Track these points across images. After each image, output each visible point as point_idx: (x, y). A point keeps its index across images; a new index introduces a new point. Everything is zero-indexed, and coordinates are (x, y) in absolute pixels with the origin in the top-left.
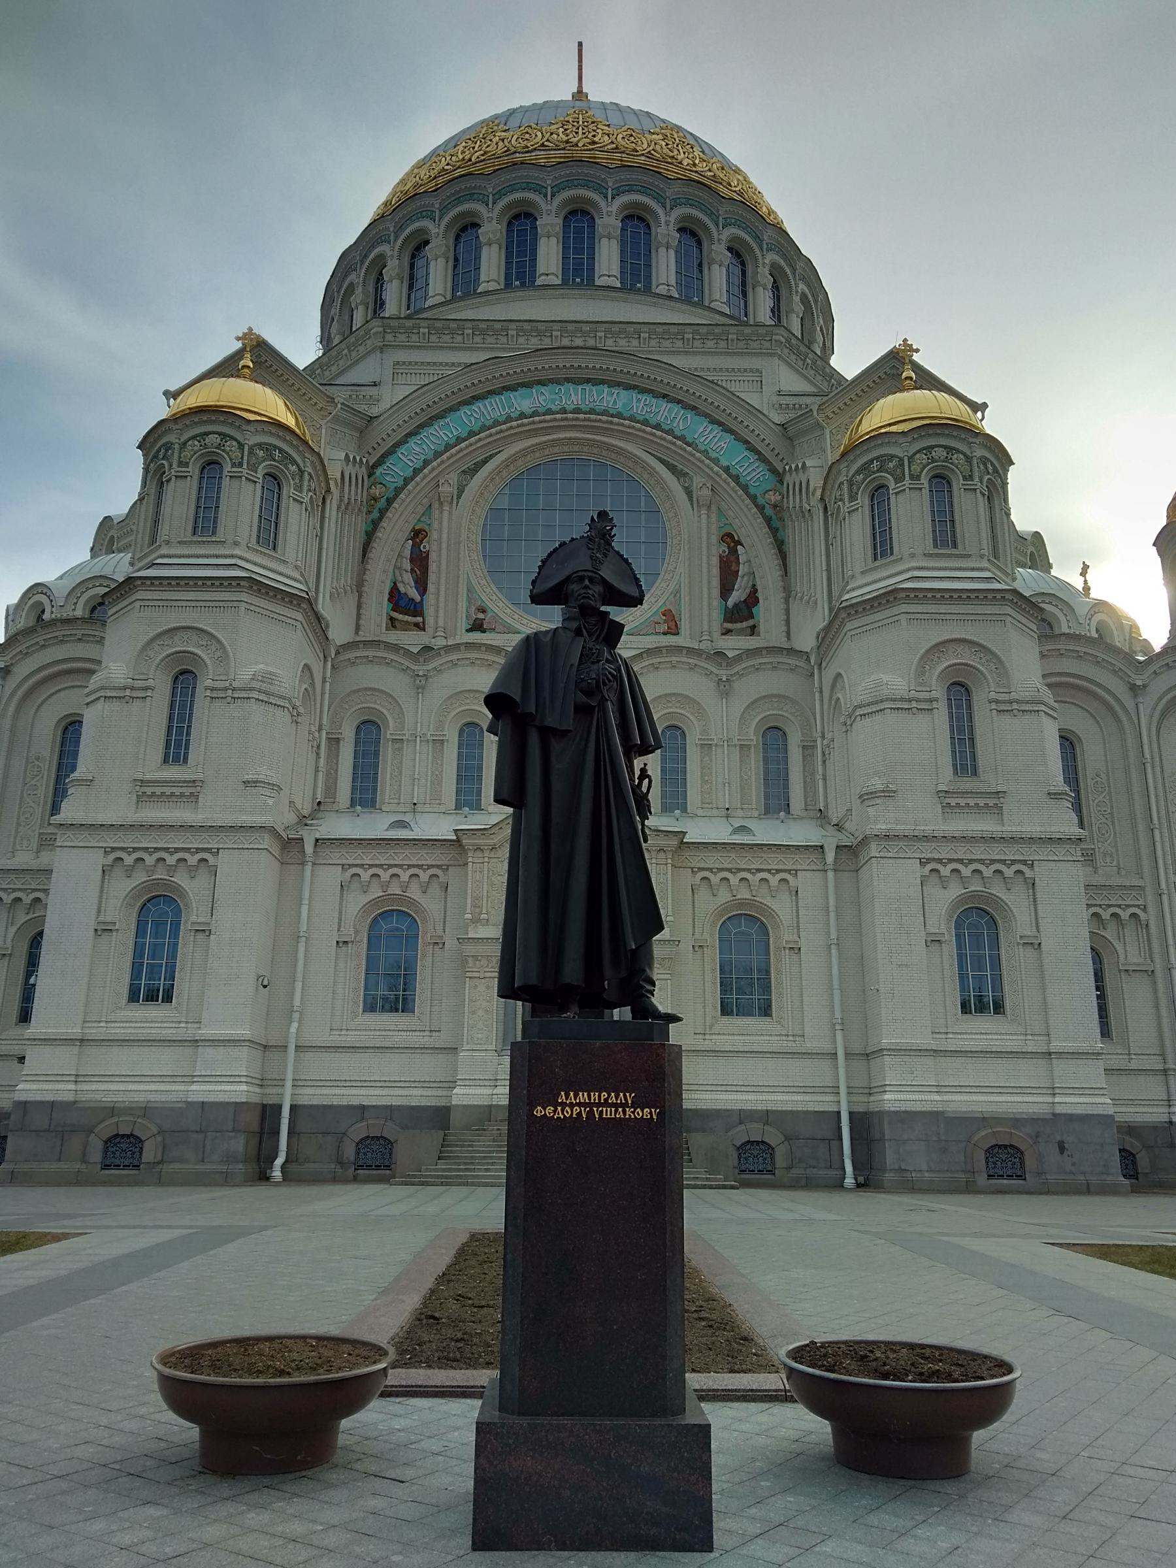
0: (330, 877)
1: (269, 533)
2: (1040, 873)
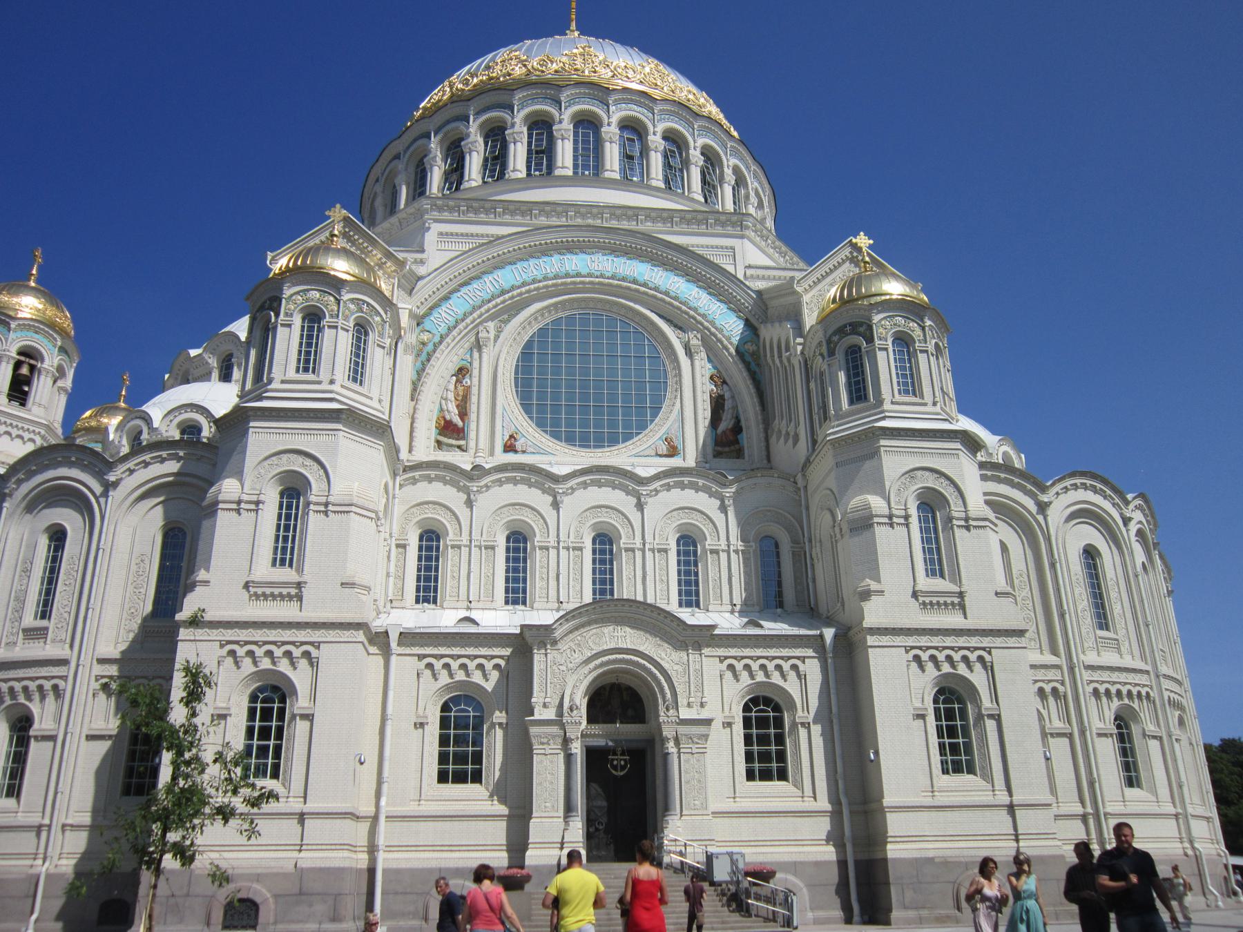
1: (357, 373)
2: (998, 657)
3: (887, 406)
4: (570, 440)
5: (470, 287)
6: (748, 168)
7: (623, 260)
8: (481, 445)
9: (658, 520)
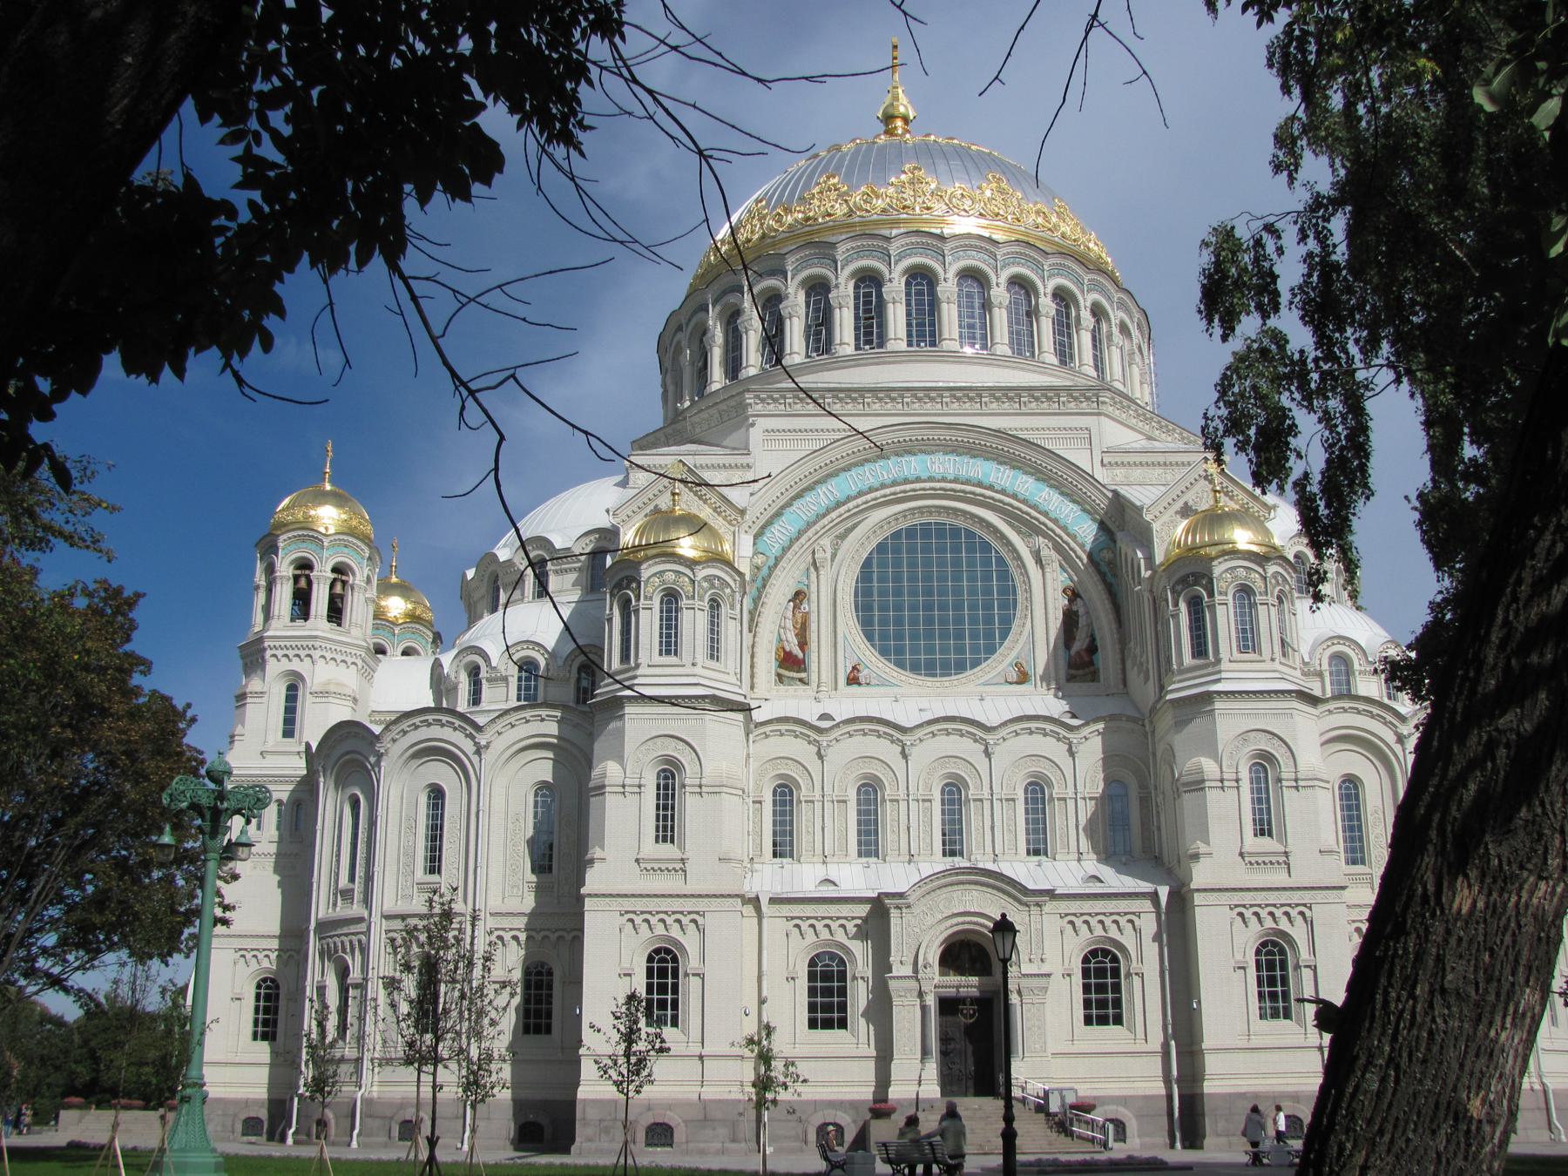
1: (714, 652)
2: (1317, 913)
3: (1225, 665)
4: (915, 668)
5: (802, 501)
6: (1109, 299)
7: (966, 459)
8: (823, 678)
9: (1002, 774)
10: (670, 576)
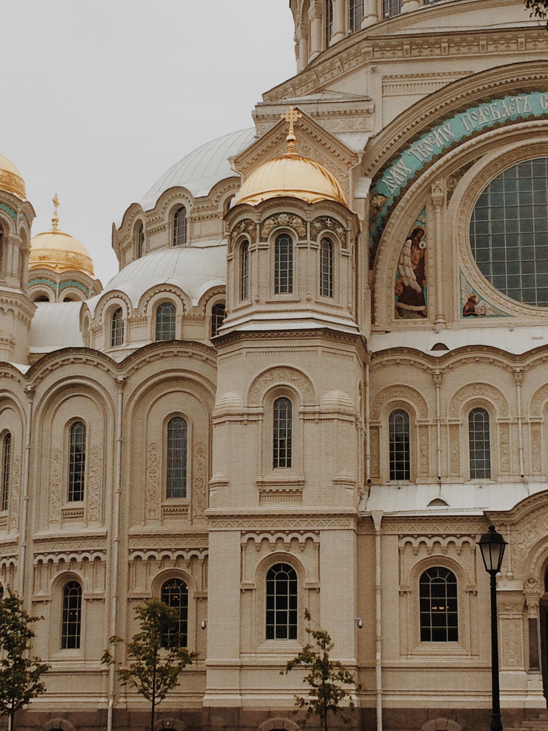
0: (392, 544)
1: (327, 287)
4: (529, 298)
5: (419, 143)
10: (283, 218)
